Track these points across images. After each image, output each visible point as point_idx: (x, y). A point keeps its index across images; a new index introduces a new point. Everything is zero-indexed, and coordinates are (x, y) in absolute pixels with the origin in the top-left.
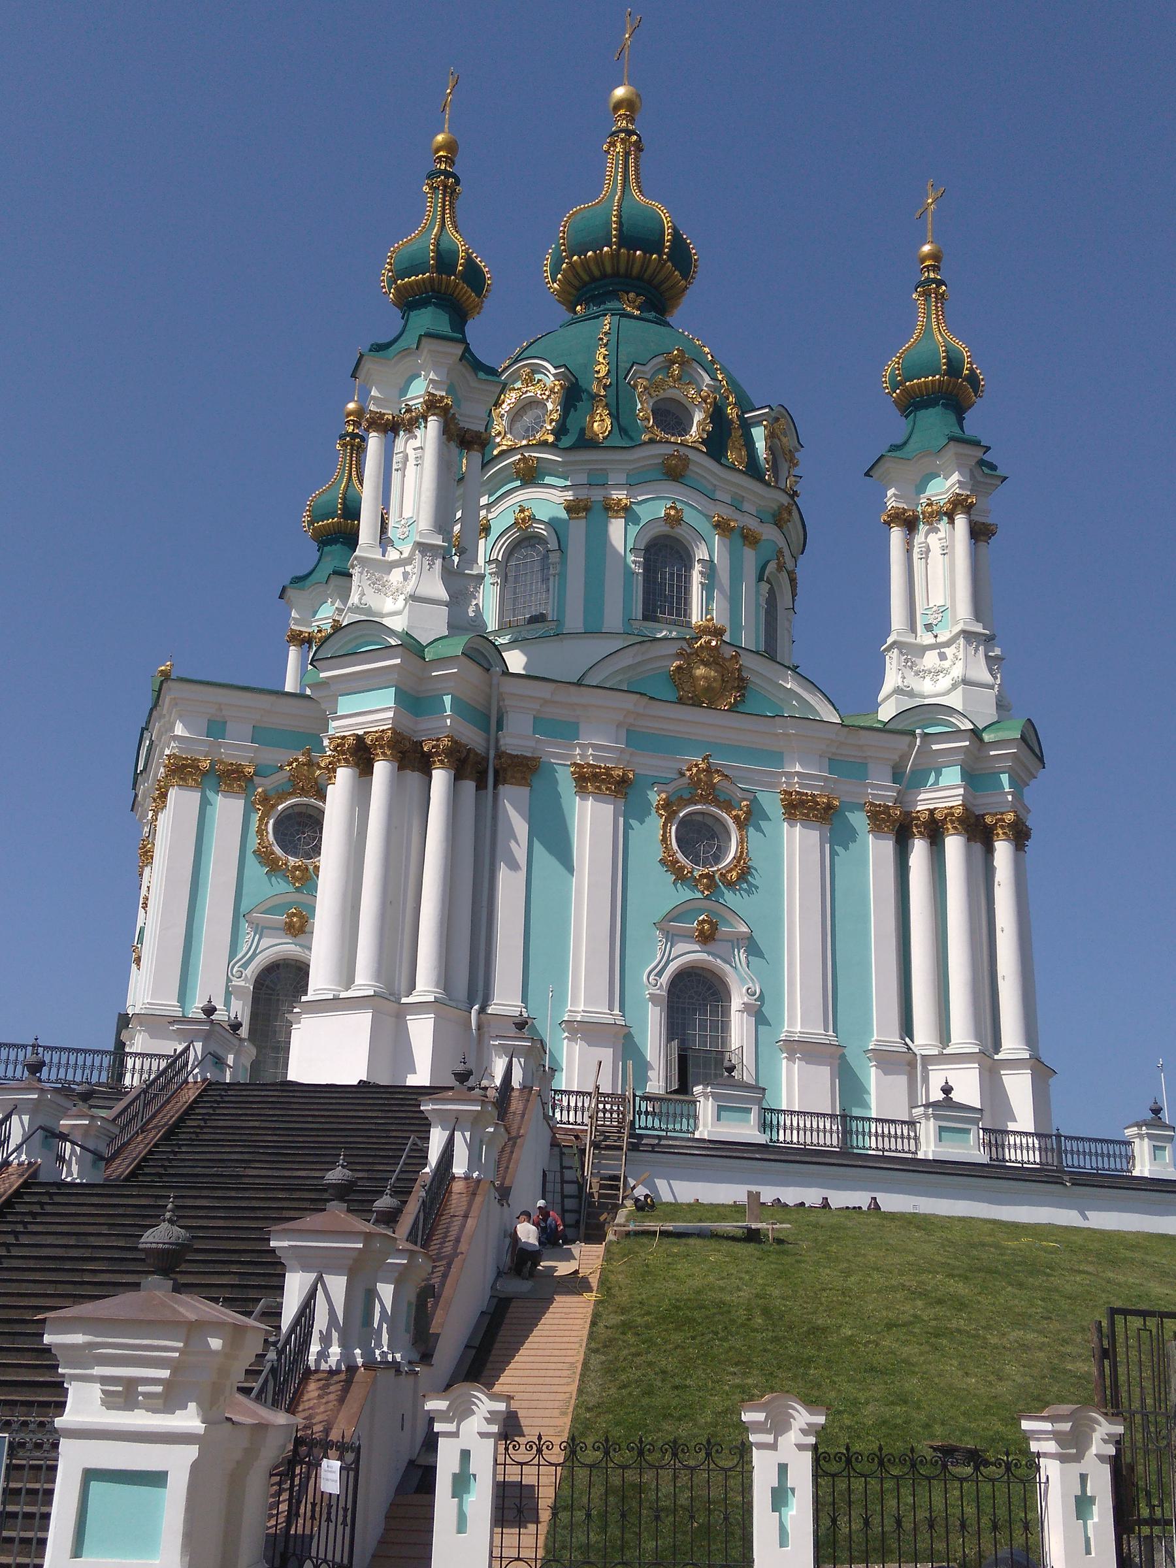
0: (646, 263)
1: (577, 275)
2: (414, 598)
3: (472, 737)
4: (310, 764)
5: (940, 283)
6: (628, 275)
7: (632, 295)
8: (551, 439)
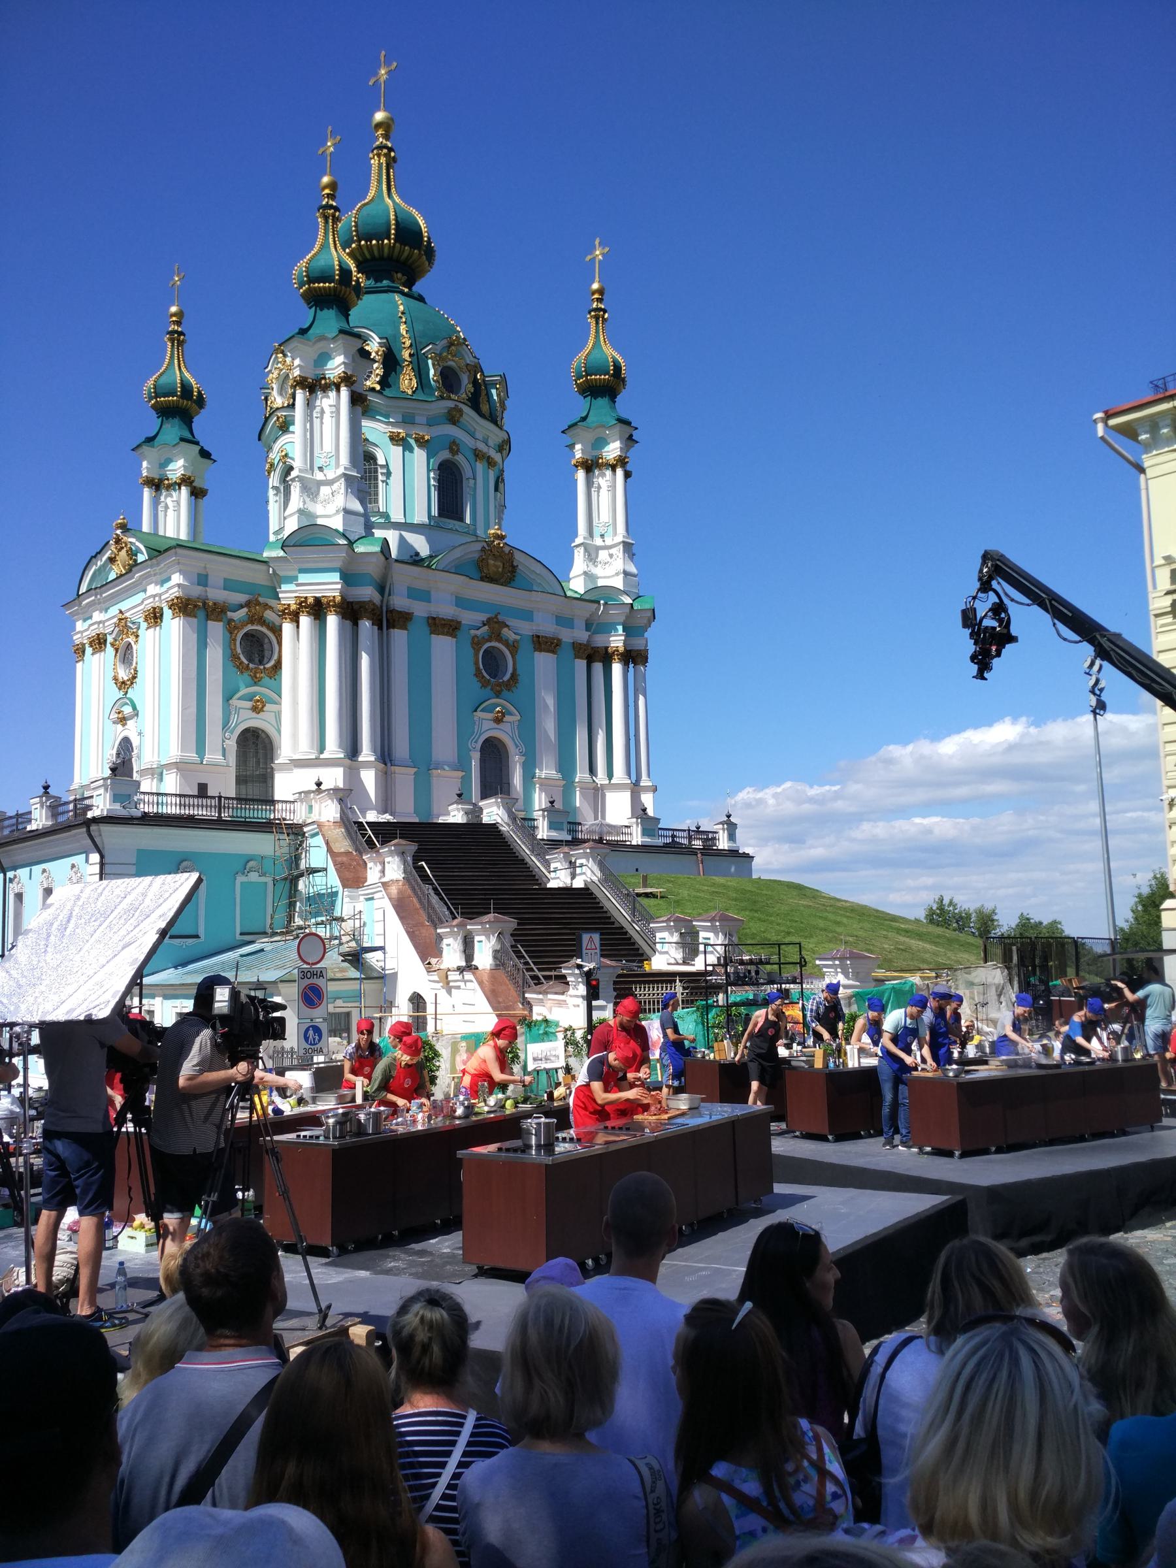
0: (410, 256)
1: (363, 254)
2: (347, 512)
3: (376, 598)
4: (258, 603)
5: (605, 311)
6: (398, 261)
7: (399, 275)
8: (378, 387)
